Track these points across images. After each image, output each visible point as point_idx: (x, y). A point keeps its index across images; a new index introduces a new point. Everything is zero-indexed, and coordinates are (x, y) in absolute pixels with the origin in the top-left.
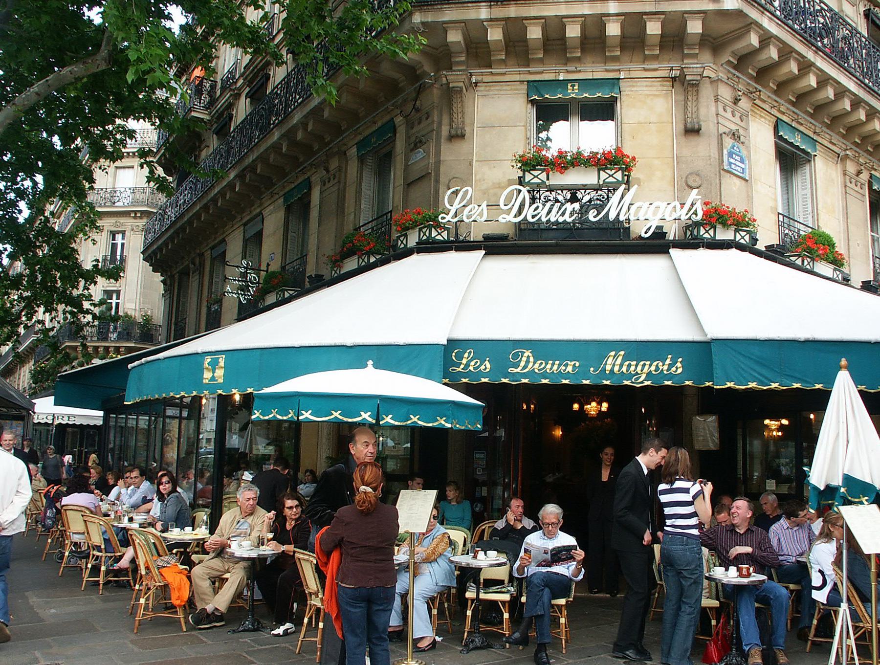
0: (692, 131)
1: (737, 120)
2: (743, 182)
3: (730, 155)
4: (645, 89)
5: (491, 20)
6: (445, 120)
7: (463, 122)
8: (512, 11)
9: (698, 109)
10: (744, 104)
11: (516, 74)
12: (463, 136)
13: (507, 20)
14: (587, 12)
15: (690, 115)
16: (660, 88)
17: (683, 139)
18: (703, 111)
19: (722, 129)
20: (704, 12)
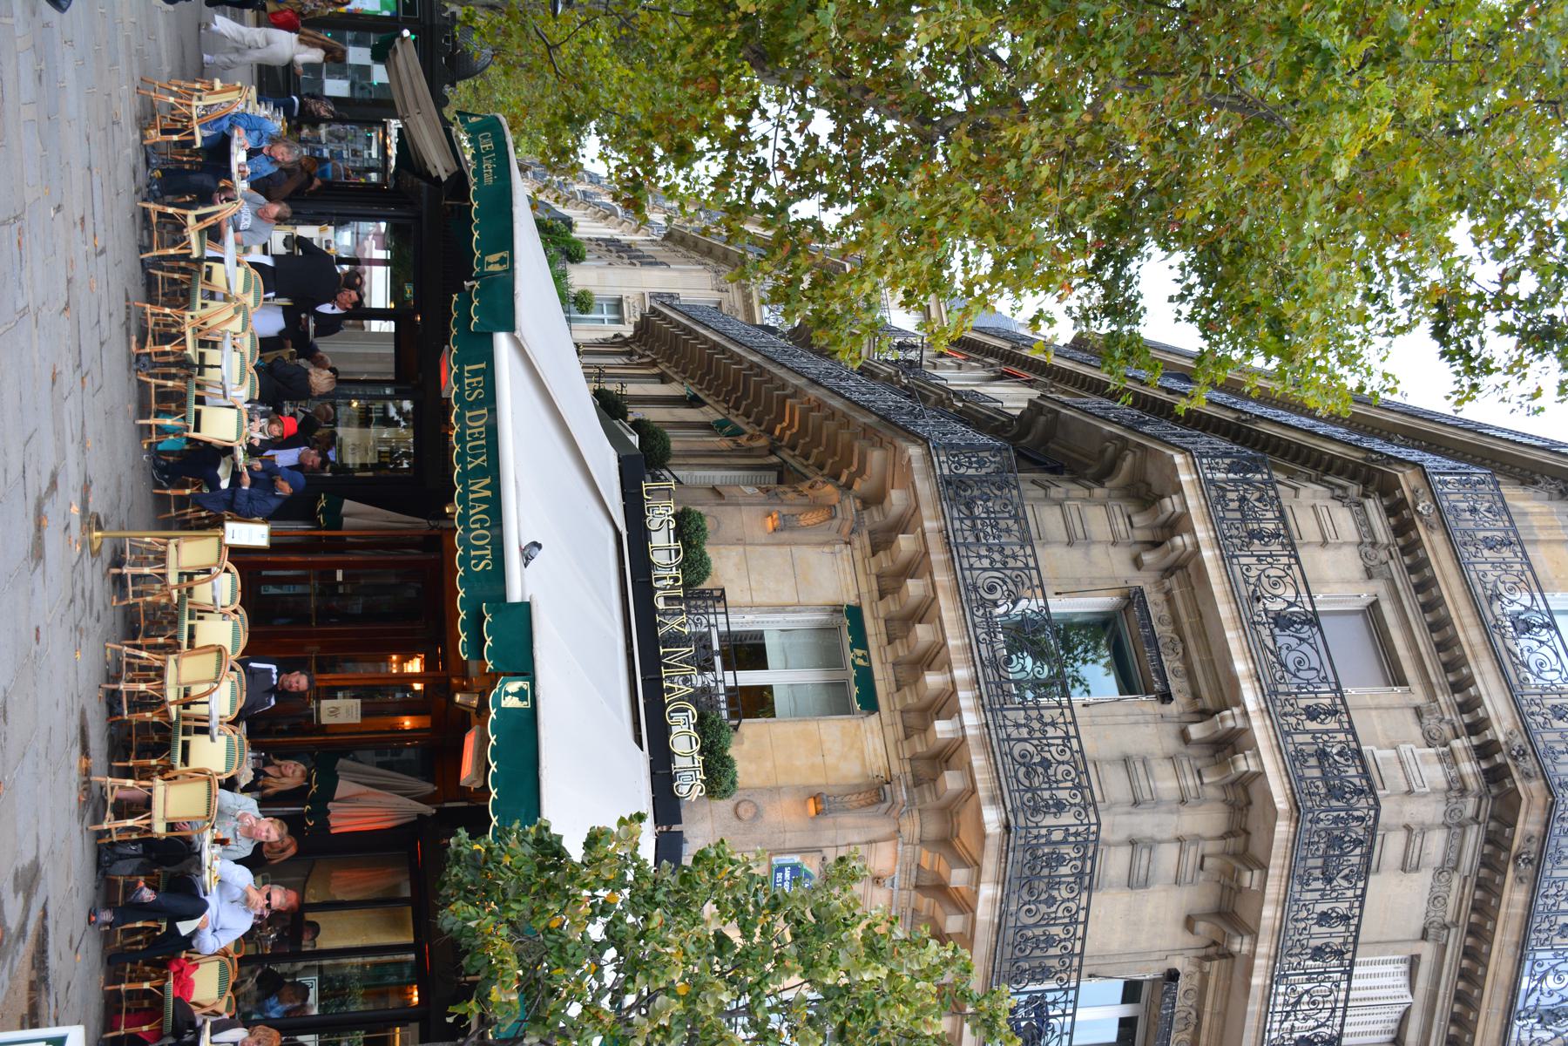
3: (795, 869)
5: (924, 534)
8: (937, 556)
11: (868, 587)
13: (927, 553)
14: (951, 643)
18: (847, 820)
20: (974, 791)
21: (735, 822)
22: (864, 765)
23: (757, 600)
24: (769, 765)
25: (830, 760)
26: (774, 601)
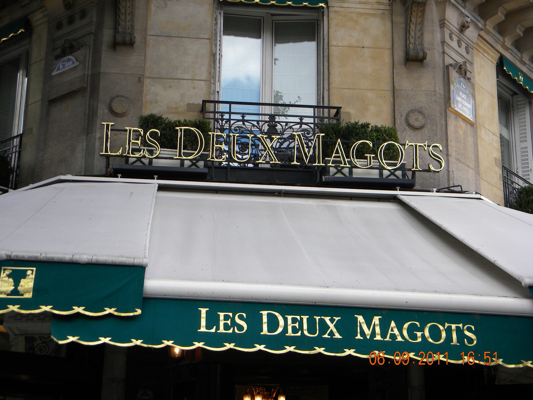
0: (414, 59)
1: (462, 51)
2: (469, 127)
4: (358, 6)
6: (108, 21)
7: (132, 27)
9: (422, 34)
10: (471, 33)
12: (131, 44)
15: (412, 40)
16: (376, 6)
17: (401, 69)
18: (427, 37)
19: (448, 61)
21: (425, 131)
22: (373, 15)
23: (204, 76)
24: (370, 95)
25: (367, 42)
26: (206, 61)
